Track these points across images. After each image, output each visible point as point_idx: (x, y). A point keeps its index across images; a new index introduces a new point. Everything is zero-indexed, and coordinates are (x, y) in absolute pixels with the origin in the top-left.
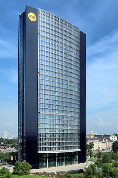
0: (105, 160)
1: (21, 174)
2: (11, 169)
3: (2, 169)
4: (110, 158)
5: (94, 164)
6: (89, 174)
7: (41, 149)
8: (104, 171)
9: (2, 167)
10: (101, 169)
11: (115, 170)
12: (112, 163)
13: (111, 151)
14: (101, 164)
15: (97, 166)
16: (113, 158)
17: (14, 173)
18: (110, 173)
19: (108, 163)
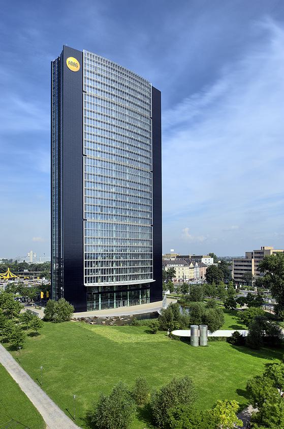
0: (194, 297)
1: (58, 321)
2: (41, 313)
3: (25, 313)
4: (203, 293)
5: (176, 303)
6: (168, 320)
7: (88, 265)
8: (192, 315)
9: (26, 310)
10: (187, 311)
11: (211, 313)
12: (206, 301)
13: (204, 282)
14: (187, 303)
15: (182, 306)
16: (207, 294)
17: (45, 320)
18: (202, 317)
19: (199, 301)
